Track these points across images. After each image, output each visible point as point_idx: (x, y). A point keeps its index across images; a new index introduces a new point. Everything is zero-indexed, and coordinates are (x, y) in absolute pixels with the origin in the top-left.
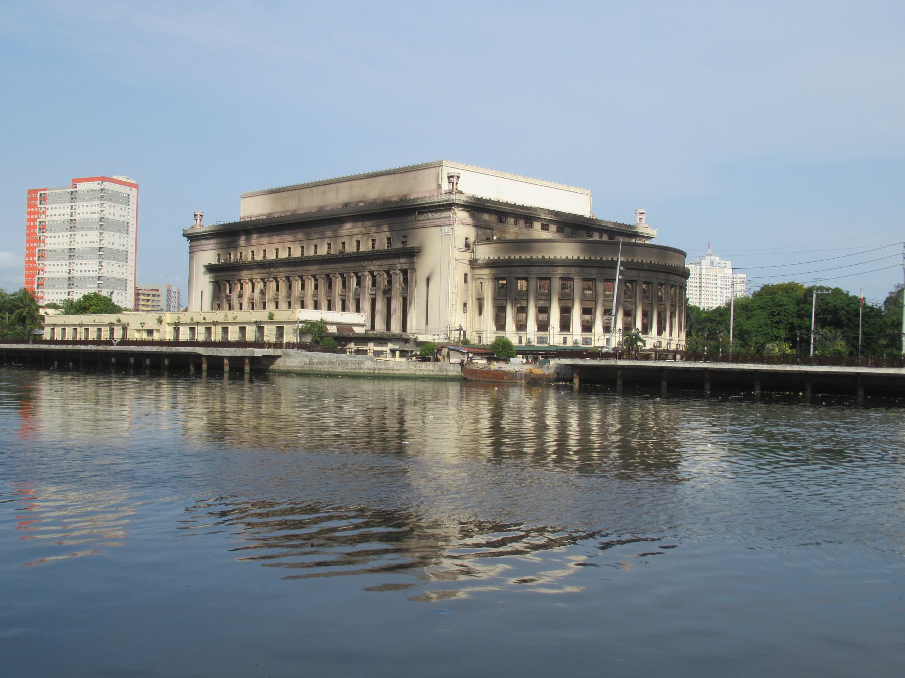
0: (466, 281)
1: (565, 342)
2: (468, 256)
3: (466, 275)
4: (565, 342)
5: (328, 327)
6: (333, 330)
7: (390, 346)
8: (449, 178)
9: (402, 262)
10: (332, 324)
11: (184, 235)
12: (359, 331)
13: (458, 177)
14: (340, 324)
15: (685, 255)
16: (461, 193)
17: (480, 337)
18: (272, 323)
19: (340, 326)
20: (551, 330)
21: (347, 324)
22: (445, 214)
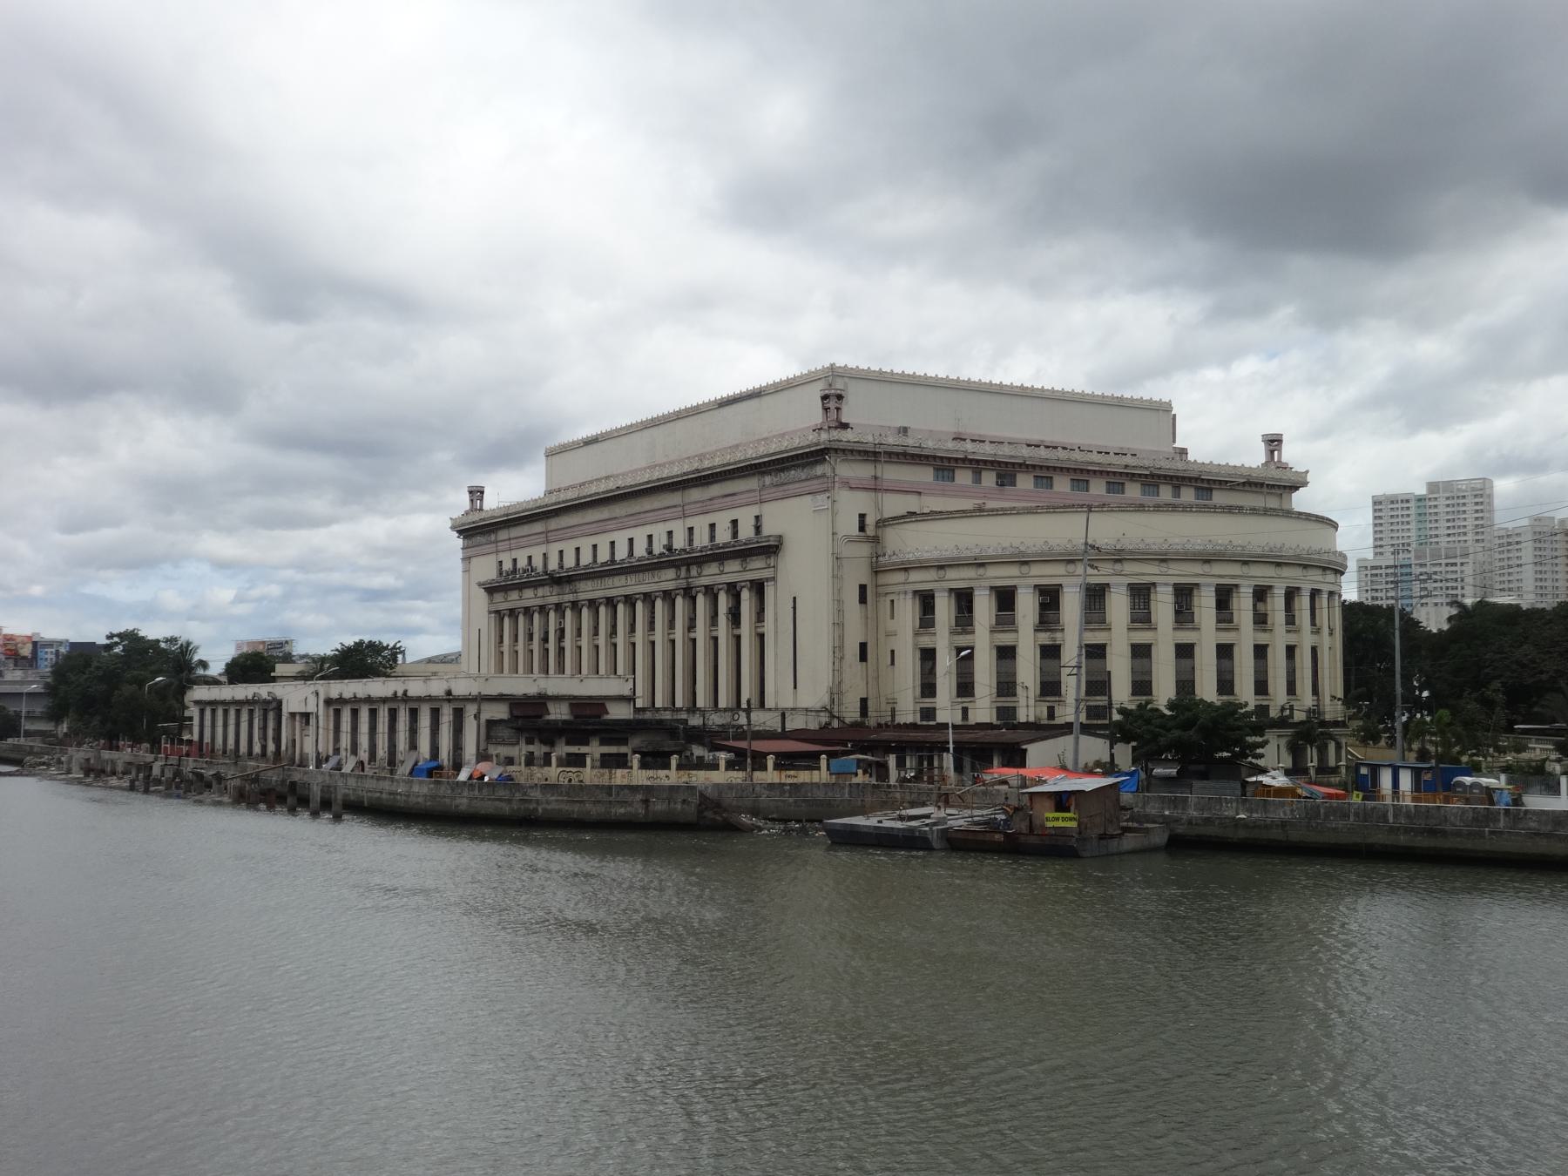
0: (863, 599)
1: (1051, 715)
2: (865, 550)
3: (863, 588)
4: (1051, 715)
5: (551, 707)
6: (559, 713)
7: (635, 742)
8: (825, 398)
9: (757, 568)
10: (558, 699)
11: (453, 528)
12: (618, 712)
13: (840, 397)
14: (575, 697)
15: (1335, 526)
16: (845, 426)
17: (893, 710)
18: (449, 701)
19: (577, 703)
20: (1019, 690)
21: (590, 698)
22: (819, 470)
